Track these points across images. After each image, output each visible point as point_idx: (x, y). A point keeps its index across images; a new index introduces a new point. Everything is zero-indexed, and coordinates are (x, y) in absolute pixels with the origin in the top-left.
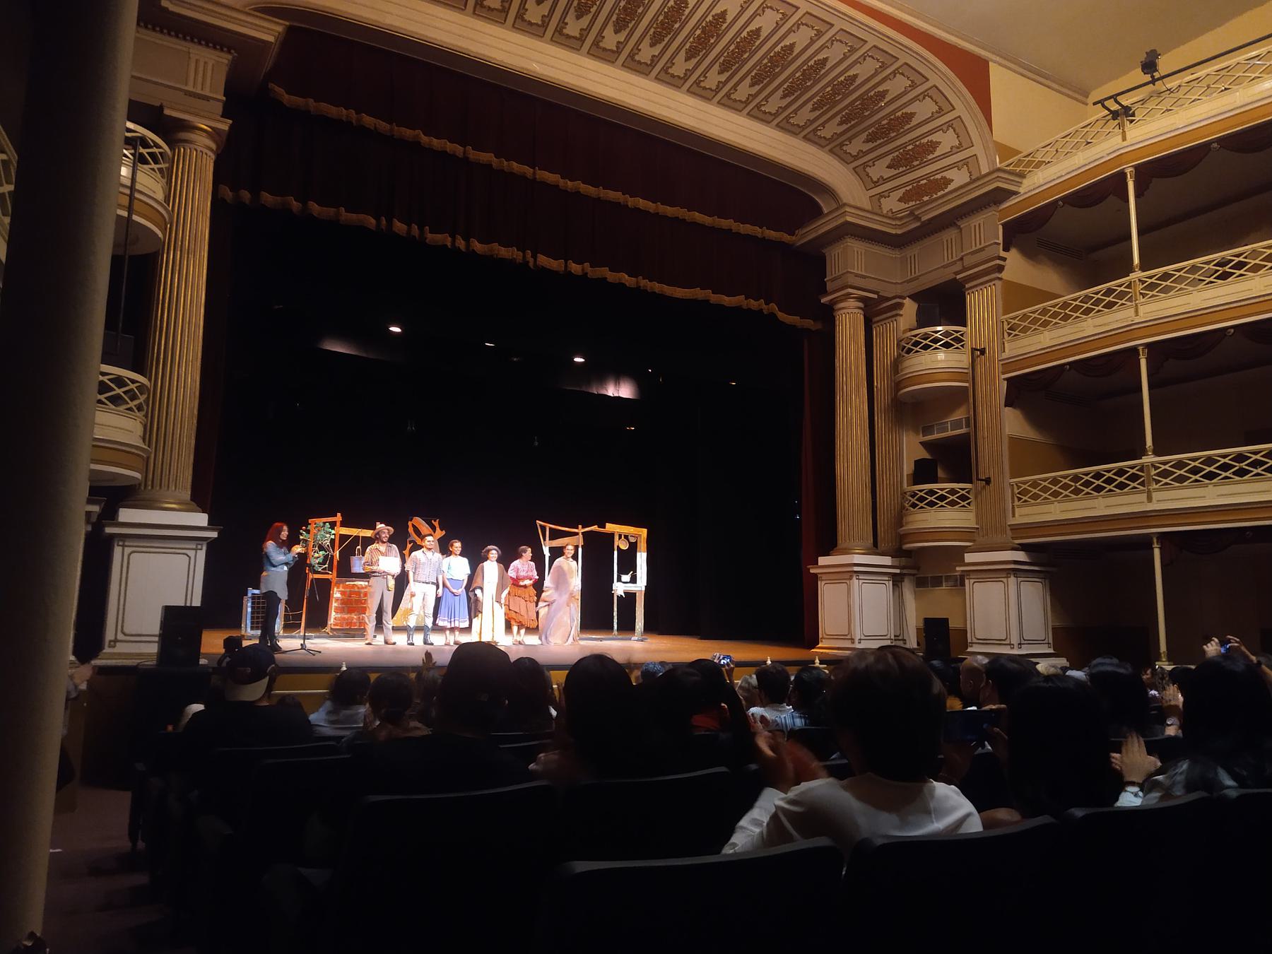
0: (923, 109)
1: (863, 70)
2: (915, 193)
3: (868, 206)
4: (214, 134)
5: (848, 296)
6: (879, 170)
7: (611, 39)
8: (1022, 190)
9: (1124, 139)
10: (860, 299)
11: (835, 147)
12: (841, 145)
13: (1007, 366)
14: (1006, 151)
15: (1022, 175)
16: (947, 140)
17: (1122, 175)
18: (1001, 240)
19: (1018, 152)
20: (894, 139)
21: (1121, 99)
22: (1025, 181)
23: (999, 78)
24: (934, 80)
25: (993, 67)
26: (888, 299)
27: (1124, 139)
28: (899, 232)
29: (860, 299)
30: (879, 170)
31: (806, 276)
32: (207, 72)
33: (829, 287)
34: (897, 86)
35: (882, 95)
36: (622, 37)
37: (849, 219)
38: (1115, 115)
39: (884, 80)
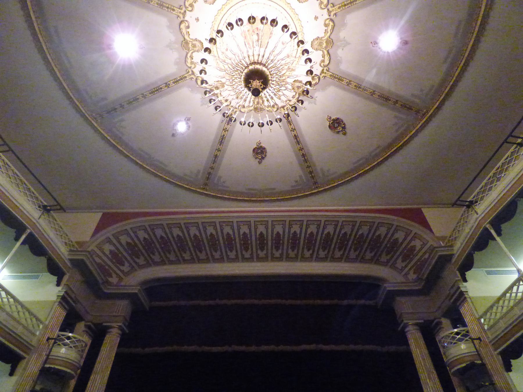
0: (400, 236)
1: (365, 230)
2: (418, 269)
3: (403, 280)
4: (120, 328)
5: (406, 325)
6: (400, 264)
7: (262, 254)
8: (455, 252)
9: (477, 214)
10: (416, 324)
11: (376, 260)
12: (378, 260)
13: (496, 344)
14: (443, 238)
15: (452, 246)
16: (417, 243)
17: (486, 229)
18: (460, 278)
19: (447, 237)
20: (397, 250)
21: (461, 199)
22: (454, 248)
23: (428, 213)
24: (395, 223)
25: (423, 209)
26: (433, 321)
27: (477, 214)
28: (420, 288)
29: (413, 325)
30: (400, 264)
31: (384, 320)
32: (123, 308)
33: (399, 321)
34: (383, 231)
35: (379, 236)
36: (265, 252)
37: (388, 289)
38: (468, 207)
39: (358, 230)
